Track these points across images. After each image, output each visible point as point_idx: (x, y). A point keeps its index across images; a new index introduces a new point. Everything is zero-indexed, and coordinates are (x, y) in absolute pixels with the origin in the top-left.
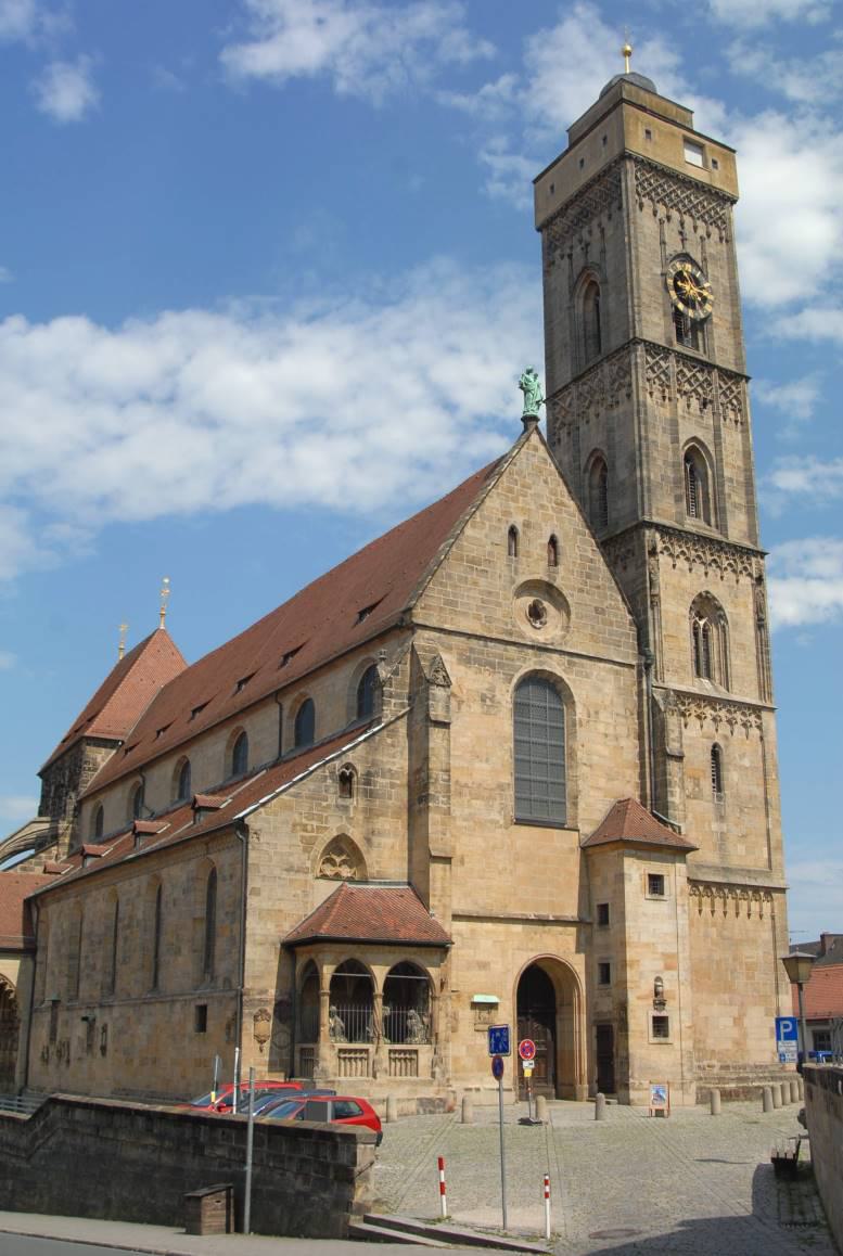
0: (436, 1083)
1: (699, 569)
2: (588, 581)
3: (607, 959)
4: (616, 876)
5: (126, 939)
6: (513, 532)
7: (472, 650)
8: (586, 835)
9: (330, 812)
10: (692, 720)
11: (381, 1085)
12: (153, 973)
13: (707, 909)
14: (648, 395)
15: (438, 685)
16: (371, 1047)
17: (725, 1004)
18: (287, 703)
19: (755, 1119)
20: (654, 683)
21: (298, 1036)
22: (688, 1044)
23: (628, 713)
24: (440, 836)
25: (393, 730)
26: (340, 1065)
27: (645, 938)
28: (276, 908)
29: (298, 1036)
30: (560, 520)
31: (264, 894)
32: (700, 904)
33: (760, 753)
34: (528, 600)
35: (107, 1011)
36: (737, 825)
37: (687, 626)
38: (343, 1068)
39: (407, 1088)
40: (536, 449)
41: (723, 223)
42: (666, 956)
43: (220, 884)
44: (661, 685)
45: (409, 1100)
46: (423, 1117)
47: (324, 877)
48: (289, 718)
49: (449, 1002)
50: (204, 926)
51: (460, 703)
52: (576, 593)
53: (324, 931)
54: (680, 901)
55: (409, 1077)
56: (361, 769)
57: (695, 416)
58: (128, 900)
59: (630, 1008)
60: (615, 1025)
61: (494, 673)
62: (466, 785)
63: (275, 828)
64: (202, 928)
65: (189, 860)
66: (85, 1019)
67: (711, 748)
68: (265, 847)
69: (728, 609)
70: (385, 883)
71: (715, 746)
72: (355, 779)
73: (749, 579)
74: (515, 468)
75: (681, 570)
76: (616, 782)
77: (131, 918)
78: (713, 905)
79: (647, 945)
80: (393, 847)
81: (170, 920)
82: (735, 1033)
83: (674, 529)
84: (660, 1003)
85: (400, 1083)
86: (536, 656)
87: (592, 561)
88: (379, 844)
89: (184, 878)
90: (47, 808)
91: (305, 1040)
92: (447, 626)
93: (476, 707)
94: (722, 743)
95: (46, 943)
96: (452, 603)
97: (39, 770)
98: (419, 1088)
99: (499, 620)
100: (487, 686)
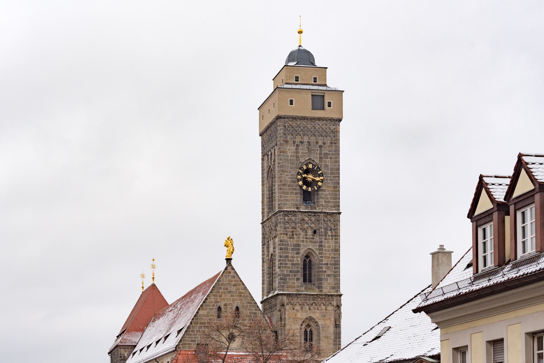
6: (219, 309)
30: (241, 300)
40: (230, 273)
41: (336, 133)
57: (309, 238)
73: (332, 307)
75: (297, 310)
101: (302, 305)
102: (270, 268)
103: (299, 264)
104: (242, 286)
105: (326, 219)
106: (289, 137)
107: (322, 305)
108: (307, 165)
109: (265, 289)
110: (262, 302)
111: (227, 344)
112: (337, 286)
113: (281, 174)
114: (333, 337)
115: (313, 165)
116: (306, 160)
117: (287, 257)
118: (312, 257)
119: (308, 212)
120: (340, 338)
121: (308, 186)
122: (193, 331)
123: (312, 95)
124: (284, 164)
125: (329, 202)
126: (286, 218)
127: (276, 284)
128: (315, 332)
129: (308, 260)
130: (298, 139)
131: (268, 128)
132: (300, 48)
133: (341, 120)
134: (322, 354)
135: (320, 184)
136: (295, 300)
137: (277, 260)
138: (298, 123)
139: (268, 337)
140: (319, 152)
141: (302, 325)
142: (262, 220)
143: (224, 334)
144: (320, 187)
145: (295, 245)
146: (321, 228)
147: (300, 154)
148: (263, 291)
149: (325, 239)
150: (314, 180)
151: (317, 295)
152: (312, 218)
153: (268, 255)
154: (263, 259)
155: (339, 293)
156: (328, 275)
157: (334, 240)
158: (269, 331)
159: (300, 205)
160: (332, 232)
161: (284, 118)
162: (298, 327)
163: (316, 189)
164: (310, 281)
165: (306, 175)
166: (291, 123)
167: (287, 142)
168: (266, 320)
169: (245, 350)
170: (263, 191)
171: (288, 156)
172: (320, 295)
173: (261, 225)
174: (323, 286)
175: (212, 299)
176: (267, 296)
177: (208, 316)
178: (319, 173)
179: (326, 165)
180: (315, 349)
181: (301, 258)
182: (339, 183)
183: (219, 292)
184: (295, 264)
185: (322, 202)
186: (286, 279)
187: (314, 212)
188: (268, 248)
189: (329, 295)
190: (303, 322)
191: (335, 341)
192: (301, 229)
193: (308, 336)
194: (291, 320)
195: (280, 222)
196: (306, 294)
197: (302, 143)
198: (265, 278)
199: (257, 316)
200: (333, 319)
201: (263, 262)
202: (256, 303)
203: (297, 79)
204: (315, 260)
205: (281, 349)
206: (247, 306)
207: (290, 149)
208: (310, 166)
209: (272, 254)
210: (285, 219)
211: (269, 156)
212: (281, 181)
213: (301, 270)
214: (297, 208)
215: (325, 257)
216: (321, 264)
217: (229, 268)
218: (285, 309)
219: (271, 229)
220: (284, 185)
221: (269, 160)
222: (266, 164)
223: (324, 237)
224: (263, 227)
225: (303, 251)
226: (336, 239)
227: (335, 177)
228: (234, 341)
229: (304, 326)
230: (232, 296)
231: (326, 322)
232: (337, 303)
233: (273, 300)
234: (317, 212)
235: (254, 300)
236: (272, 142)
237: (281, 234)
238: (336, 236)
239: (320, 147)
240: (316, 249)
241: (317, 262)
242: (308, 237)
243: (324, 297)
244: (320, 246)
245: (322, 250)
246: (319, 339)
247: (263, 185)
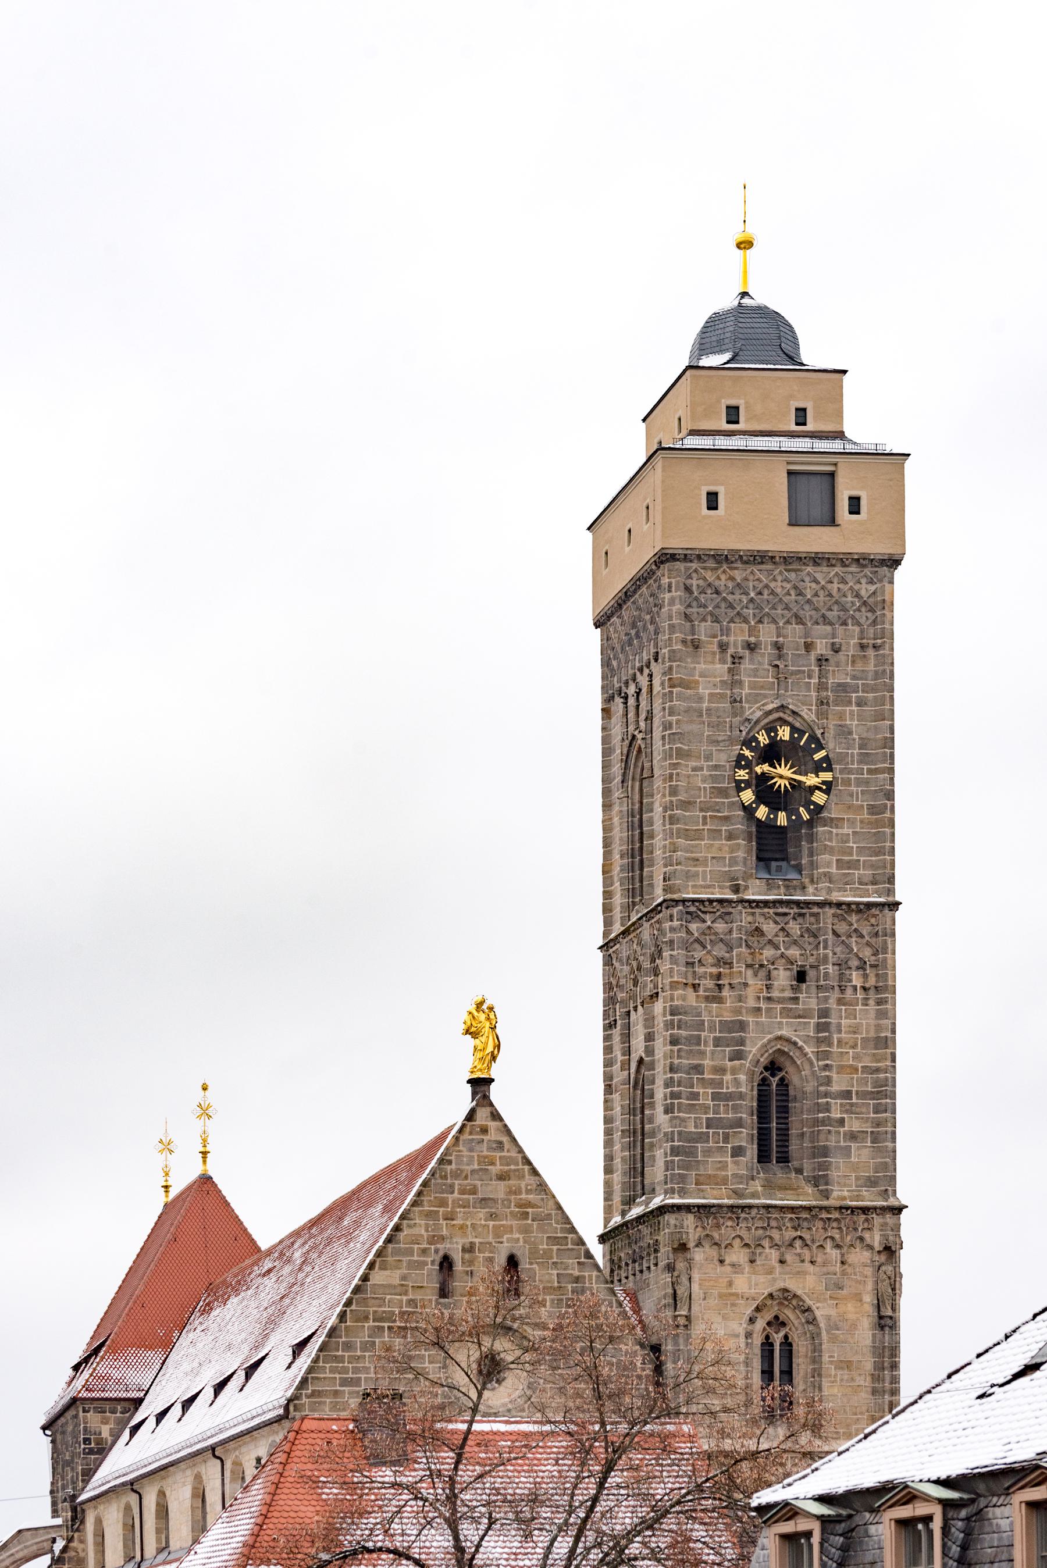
6: (446, 1263)
14: (690, 990)
30: (526, 1230)
40: (484, 1130)
41: (879, 610)
57: (780, 1000)
73: (867, 1254)
74: (449, 1167)
75: (733, 1265)
101: (754, 1248)
102: (632, 1112)
103: (741, 1096)
104: (530, 1180)
105: (842, 928)
106: (704, 630)
107: (829, 1244)
108: (771, 729)
109: (617, 1188)
110: (603, 1239)
111: (474, 1395)
112: (884, 1176)
113: (675, 766)
114: (868, 1365)
115: (794, 729)
116: (769, 713)
117: (698, 1069)
118: (790, 1069)
119: (775, 902)
120: (895, 1366)
121: (774, 808)
123: (790, 473)
124: (686, 728)
125: (854, 865)
126: (694, 927)
127: (656, 1172)
128: (801, 1347)
129: (774, 1081)
130: (738, 636)
131: (626, 596)
132: (746, 301)
133: (894, 562)
134: (828, 1429)
135: (819, 798)
136: (727, 1230)
137: (659, 1082)
138: (738, 575)
139: (626, 1368)
140: (815, 680)
141: (752, 1320)
142: (605, 934)
143: (461, 1358)
144: (820, 808)
145: (726, 1026)
146: (825, 960)
147: (746, 690)
148: (608, 1197)
149: (840, 1001)
150: (796, 785)
151: (809, 1209)
152: (792, 924)
153: (626, 1065)
154: (608, 1078)
155: (892, 1202)
156: (853, 1136)
157: (872, 1006)
158: (628, 1346)
159: (746, 877)
160: (865, 976)
161: (686, 558)
162: (739, 1327)
163: (806, 816)
164: (784, 1159)
165: (766, 767)
166: (710, 576)
167: (696, 646)
168: (620, 1304)
169: (538, 1416)
170: (607, 828)
171: (700, 699)
172: (821, 1208)
173: (600, 955)
174: (834, 1174)
175: (419, 1227)
176: (623, 1213)
178: (817, 756)
179: (841, 729)
180: (800, 1411)
181: (751, 1074)
182: (890, 795)
183: (443, 1203)
184: (729, 1097)
185: (829, 864)
186: (691, 1153)
187: (798, 903)
188: (627, 1037)
189: (853, 1210)
190: (758, 1309)
191: (876, 1378)
192: (748, 966)
193: (777, 1361)
194: (713, 1302)
195: (672, 942)
196: (768, 1207)
197: (751, 647)
198: (617, 1147)
199: (583, 1291)
200: (868, 1298)
201: (609, 1089)
202: (581, 1242)
203: (733, 414)
204: (802, 1079)
205: (672, 1413)
206: (547, 1254)
207: (709, 673)
208: (784, 733)
209: (641, 1061)
210: (689, 932)
211: (631, 701)
212: (674, 791)
213: (750, 1120)
214: (736, 889)
215: (841, 1069)
216: (826, 1095)
217: (482, 1114)
218: (690, 1261)
219: (639, 968)
220: (686, 805)
221: (631, 715)
222: (617, 731)
223: (836, 994)
224: (608, 962)
225: (755, 1047)
226: (879, 1003)
227: (876, 771)
228: (499, 1382)
229: (760, 1324)
230: (492, 1216)
231: (842, 1308)
232: (885, 1237)
233: (645, 1230)
234: (808, 904)
235: (573, 1230)
236: (641, 647)
237: (674, 985)
238: (882, 991)
239: (821, 661)
240: (807, 1039)
241: (809, 1088)
242: (775, 994)
243: (836, 1215)
244: (821, 1027)
245: (828, 1041)
246: (817, 1373)
247: (607, 806)
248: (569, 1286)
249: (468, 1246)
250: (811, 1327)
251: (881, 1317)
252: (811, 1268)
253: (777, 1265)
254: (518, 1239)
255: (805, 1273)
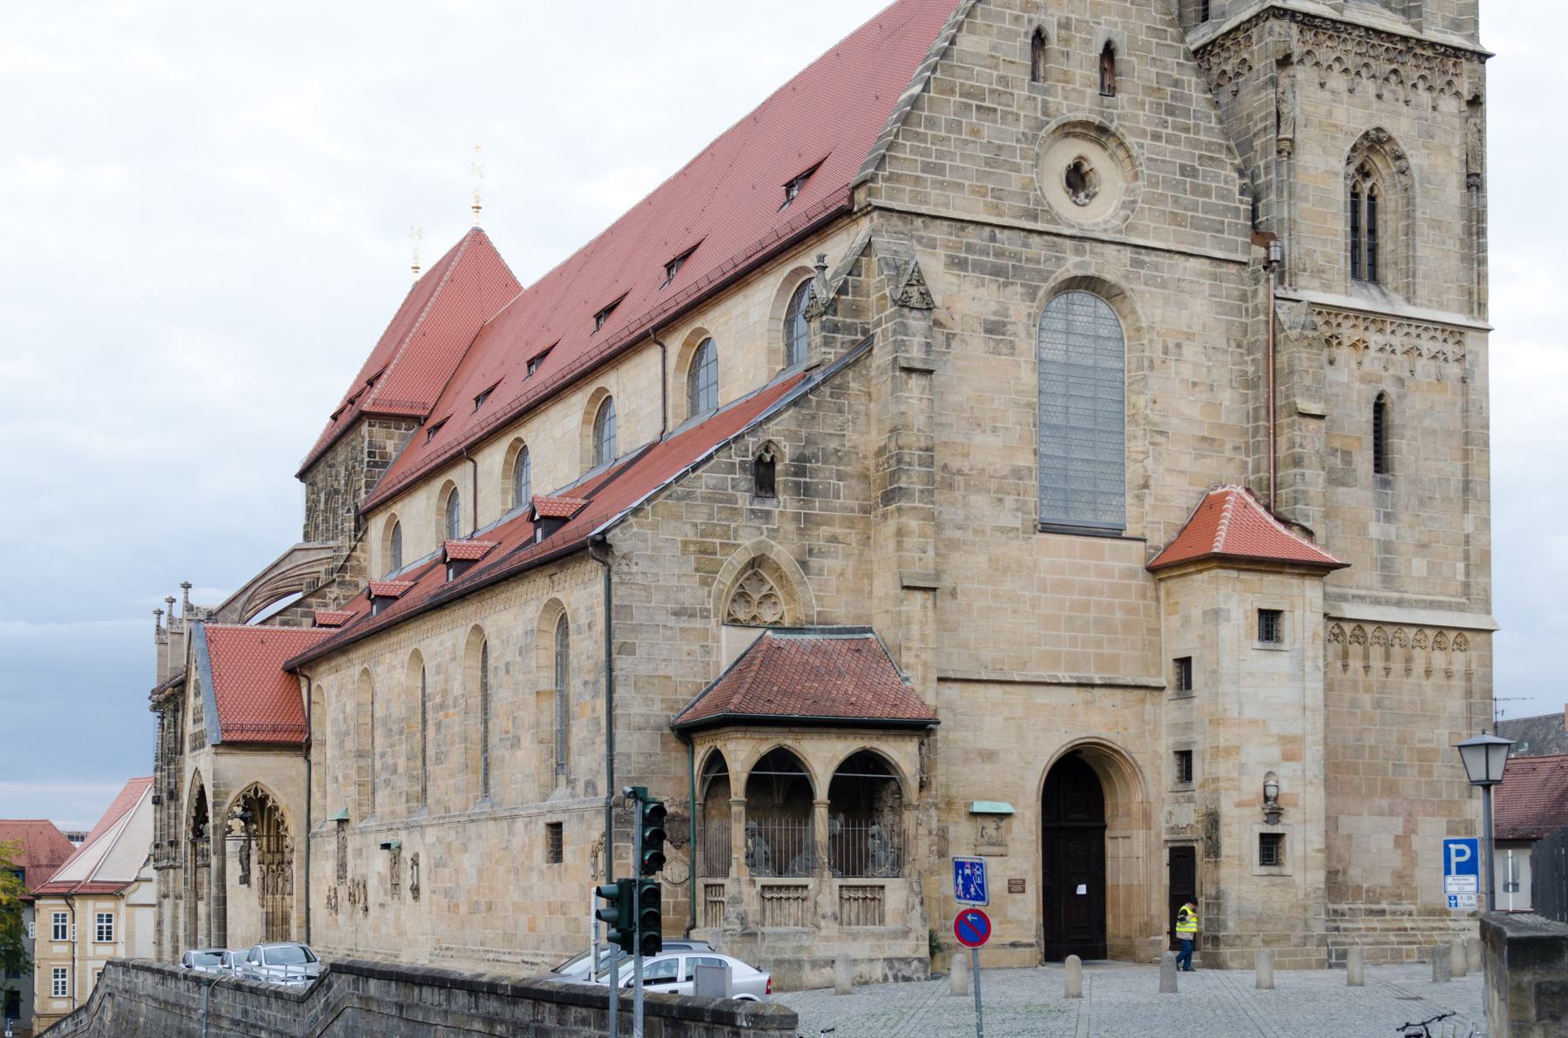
0: (912, 935)
1: (1368, 87)
2: (1170, 119)
3: (1188, 744)
4: (1205, 613)
5: (439, 726)
6: (1039, 39)
7: (970, 248)
8: (1157, 549)
9: (741, 521)
10: (1343, 354)
11: (827, 939)
12: (481, 777)
13: (1356, 664)
15: (912, 308)
16: (810, 882)
17: (1381, 814)
18: (675, 343)
19: (1415, 992)
20: (1280, 292)
21: (700, 868)
22: (1318, 878)
23: (1233, 344)
24: (917, 555)
25: (839, 387)
26: (763, 910)
27: (1250, 712)
28: (660, 673)
29: (700, 868)
31: (641, 652)
32: (1345, 655)
33: (1459, 405)
34: (1066, 153)
35: (416, 835)
36: (1411, 527)
37: (1341, 196)
38: (768, 913)
39: (868, 943)
42: (1285, 739)
43: (573, 637)
44: (1291, 295)
45: (871, 960)
46: (894, 986)
47: (734, 622)
48: (678, 369)
49: (933, 812)
50: (556, 700)
51: (949, 337)
52: (1147, 142)
53: (737, 704)
54: (1310, 653)
55: (870, 927)
56: (786, 452)
58: (439, 666)
59: (1223, 821)
60: (1199, 848)
61: (1006, 285)
62: (960, 472)
63: (654, 548)
64: (550, 708)
65: (526, 602)
66: (386, 846)
67: (1373, 400)
68: (639, 579)
69: (1416, 160)
70: (831, 631)
71: (1380, 396)
72: (779, 467)
76: (1208, 461)
77: (445, 693)
78: (1366, 656)
79: (1255, 722)
80: (842, 574)
81: (502, 697)
82: (1396, 860)
83: (1325, 19)
84: (1274, 814)
85: (855, 937)
86: (1077, 252)
87: (1177, 83)
88: (821, 569)
89: (519, 631)
90: (317, 527)
91: (711, 873)
92: (923, 209)
93: (975, 344)
94: (1392, 392)
95: (324, 734)
96: (940, 169)
97: (298, 468)
98: (886, 942)
99: (1014, 193)
100: (993, 307)
122: (931, 123)
136: (1325, 54)
177: (993, 62)
200: (1457, 153)
248: (1169, 89)
249: (1063, 21)
250: (1402, 178)
251: (1469, 176)
252: (1405, 109)
253: (1374, 99)
254: (1116, 24)
255: (1400, 114)
